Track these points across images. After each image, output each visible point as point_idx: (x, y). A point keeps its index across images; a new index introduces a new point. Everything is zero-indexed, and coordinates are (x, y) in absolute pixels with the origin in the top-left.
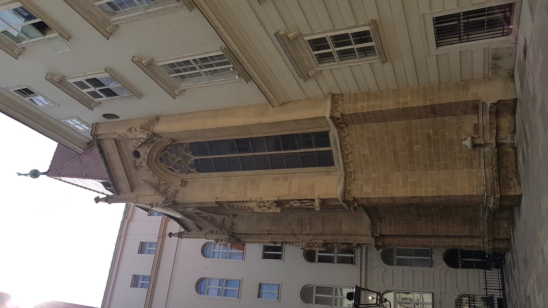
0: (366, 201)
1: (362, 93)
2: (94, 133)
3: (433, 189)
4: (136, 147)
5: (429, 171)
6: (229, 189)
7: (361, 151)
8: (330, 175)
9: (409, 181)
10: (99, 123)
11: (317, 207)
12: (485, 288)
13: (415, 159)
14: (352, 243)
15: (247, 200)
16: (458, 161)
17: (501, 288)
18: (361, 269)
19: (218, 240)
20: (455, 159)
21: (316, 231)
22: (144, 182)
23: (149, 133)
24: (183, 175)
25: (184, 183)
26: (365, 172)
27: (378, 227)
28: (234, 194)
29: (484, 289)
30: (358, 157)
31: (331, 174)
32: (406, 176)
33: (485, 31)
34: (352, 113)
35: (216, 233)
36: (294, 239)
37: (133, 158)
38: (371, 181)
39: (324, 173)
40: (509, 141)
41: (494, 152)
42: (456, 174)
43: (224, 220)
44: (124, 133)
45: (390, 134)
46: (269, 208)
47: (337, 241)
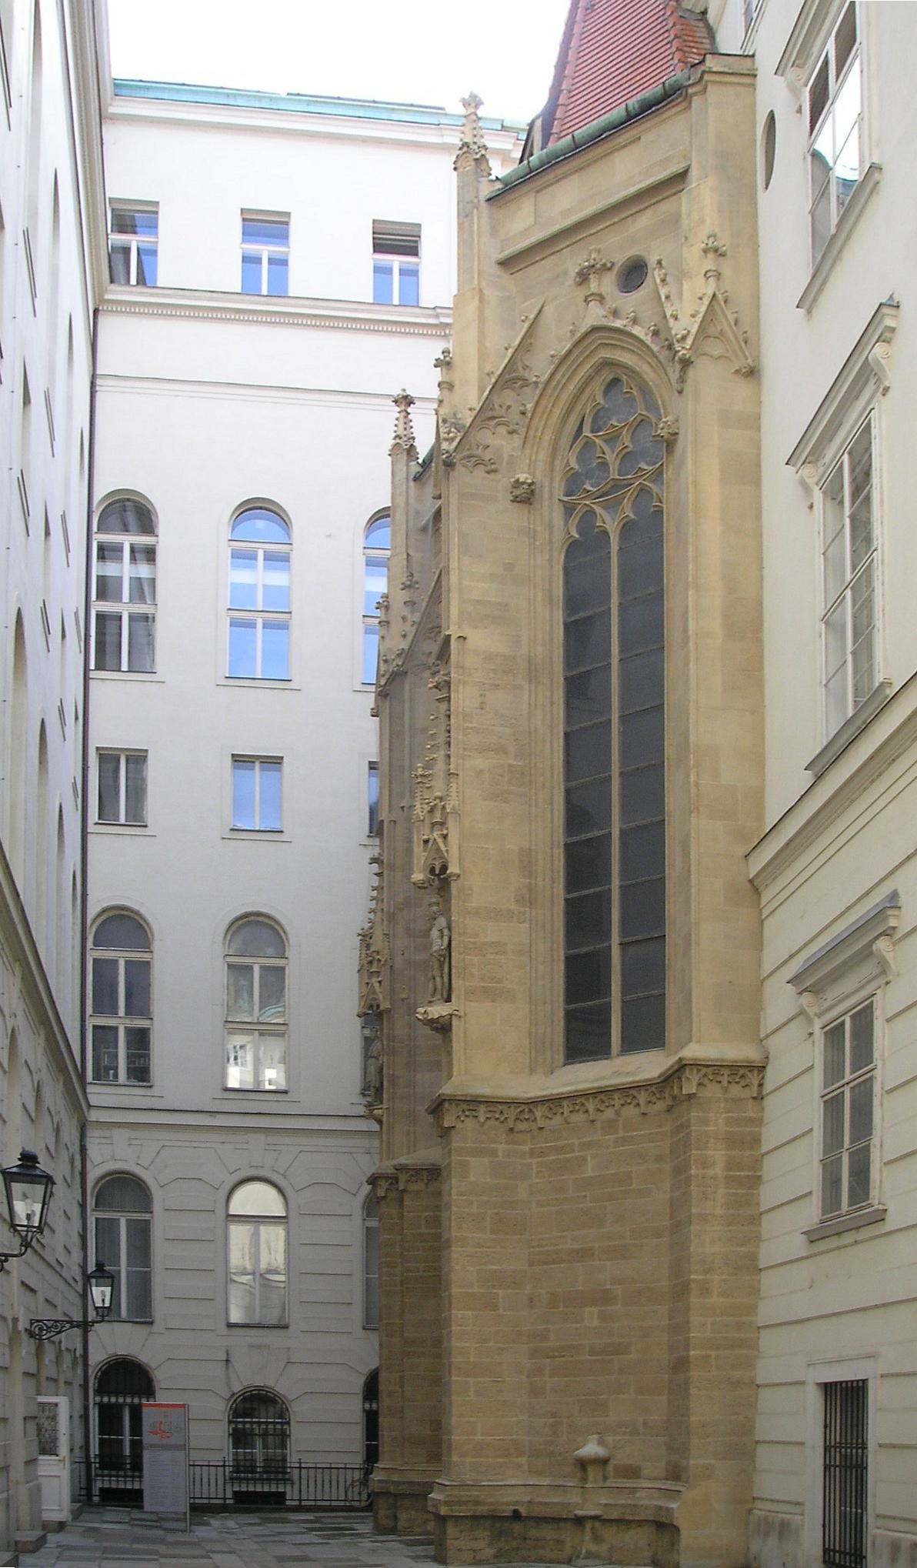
9: (500, 1291)
20: (554, 1415)
22: (532, 316)
24: (560, 485)
25: (525, 496)
26: (534, 1161)
28: (478, 705)
30: (576, 1142)
32: (514, 1283)
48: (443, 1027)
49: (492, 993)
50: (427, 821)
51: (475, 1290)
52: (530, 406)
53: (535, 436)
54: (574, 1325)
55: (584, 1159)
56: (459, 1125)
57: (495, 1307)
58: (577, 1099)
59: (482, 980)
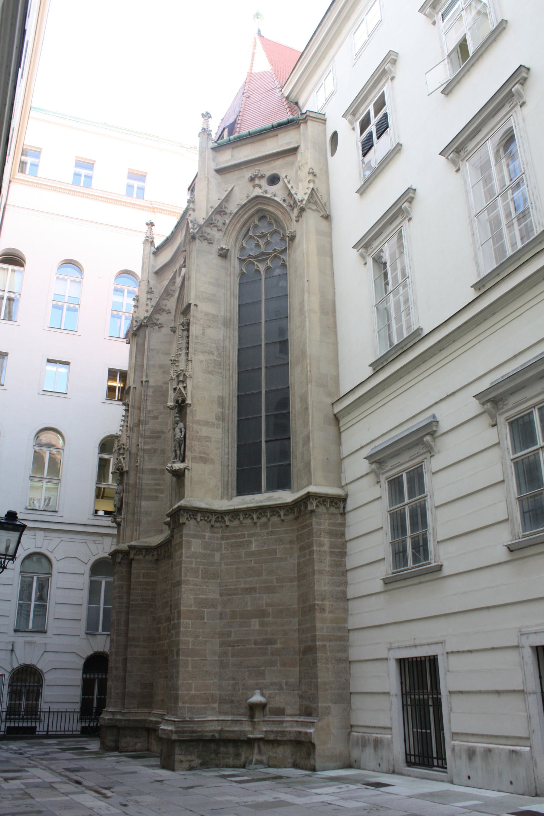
0: (178, 541)
1: (344, 544)
2: (309, 116)
3: (190, 644)
4: (285, 180)
5: (218, 640)
6: (210, 326)
7: (256, 538)
8: (223, 489)
9: (205, 610)
10: (325, 124)
11: (172, 466)
12: (51, 710)
13: (238, 620)
14: (121, 516)
15: (189, 354)
16: (232, 682)
17: (50, 733)
18: (85, 525)
19: (138, 301)
20: (234, 679)
21: (142, 460)
22: (229, 190)
23: (304, 202)
24: (238, 252)
25: (224, 254)
26: (223, 542)
27: (144, 557)
28: (201, 333)
29: (50, 709)
31: (224, 489)
32: (213, 605)
33: (415, 730)
34: (313, 528)
35: (148, 299)
36: (132, 423)
37: (268, 174)
38: (208, 552)
39: (226, 479)
40: (256, 757)
41: (241, 735)
42: (212, 679)
43: (169, 313)
44: (307, 163)
45: (278, 584)
46: (175, 389)
47: (126, 492)
48: (179, 475)
49: (204, 460)
50: (176, 380)
51: (193, 608)
52: (227, 222)
53: (229, 233)
54: (245, 629)
55: (251, 542)
56: (187, 522)
57: (203, 618)
58: (248, 512)
59: (200, 453)
